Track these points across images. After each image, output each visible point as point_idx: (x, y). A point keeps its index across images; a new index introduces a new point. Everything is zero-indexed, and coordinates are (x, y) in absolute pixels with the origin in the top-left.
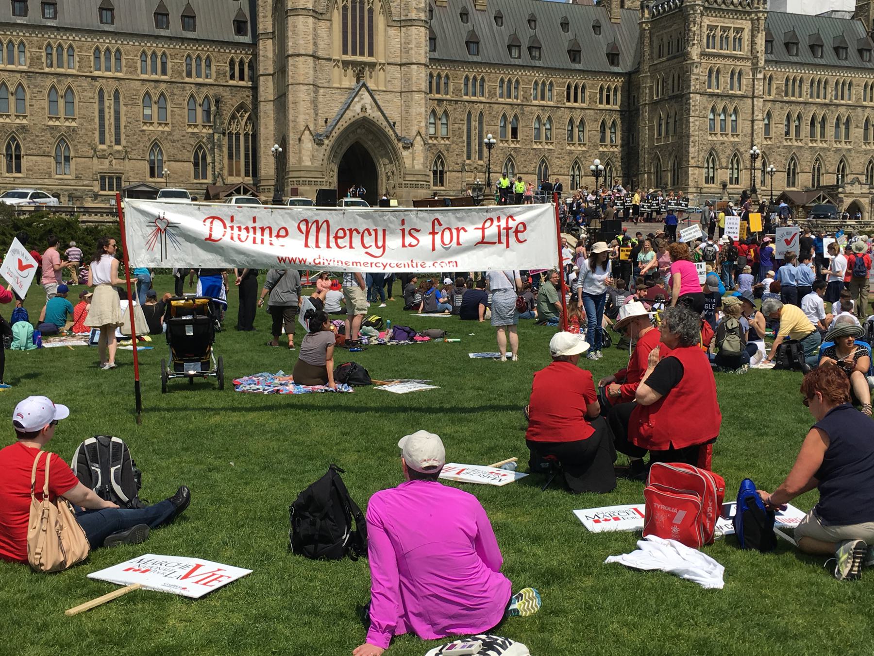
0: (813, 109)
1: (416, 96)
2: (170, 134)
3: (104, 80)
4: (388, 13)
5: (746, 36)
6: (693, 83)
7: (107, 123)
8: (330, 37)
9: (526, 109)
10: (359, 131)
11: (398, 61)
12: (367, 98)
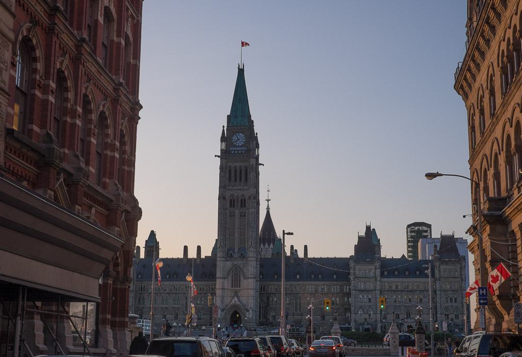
4: (244, 276)
8: (227, 284)
9: (316, 295)
12: (236, 299)
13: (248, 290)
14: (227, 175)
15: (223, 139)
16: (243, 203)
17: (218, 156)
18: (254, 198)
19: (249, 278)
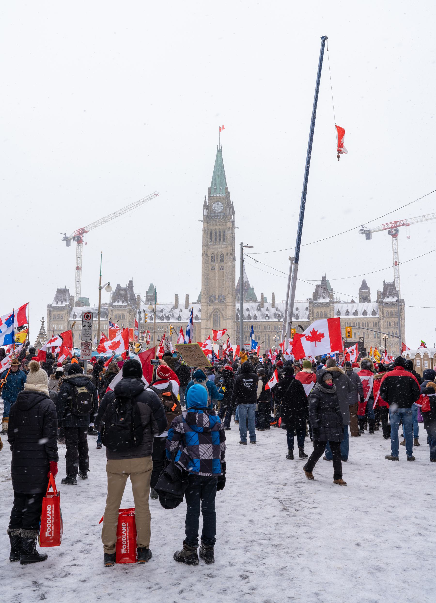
4: (223, 317)
14: (209, 236)
15: (206, 207)
16: (222, 259)
17: (202, 221)
18: (231, 254)
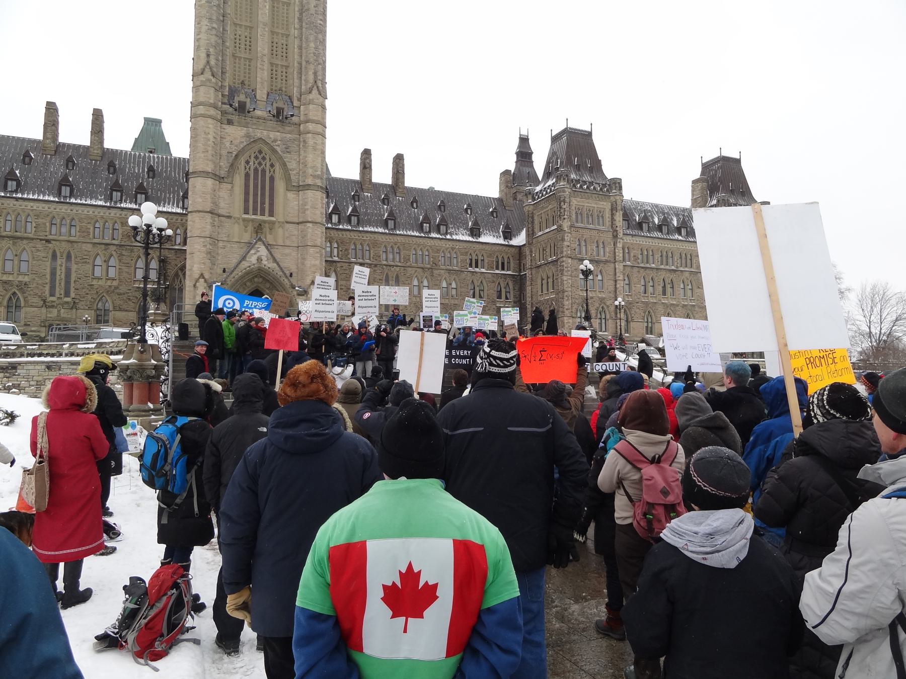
0: (663, 274)
1: (312, 250)
2: (116, 288)
3: (58, 243)
4: (288, 179)
5: (607, 214)
6: (565, 249)
7: (58, 278)
9: (436, 272)
10: (256, 280)
11: (296, 220)
12: (263, 251)
13: (300, 226)
19: (307, 187)
